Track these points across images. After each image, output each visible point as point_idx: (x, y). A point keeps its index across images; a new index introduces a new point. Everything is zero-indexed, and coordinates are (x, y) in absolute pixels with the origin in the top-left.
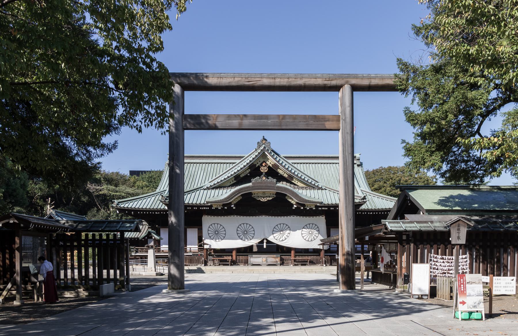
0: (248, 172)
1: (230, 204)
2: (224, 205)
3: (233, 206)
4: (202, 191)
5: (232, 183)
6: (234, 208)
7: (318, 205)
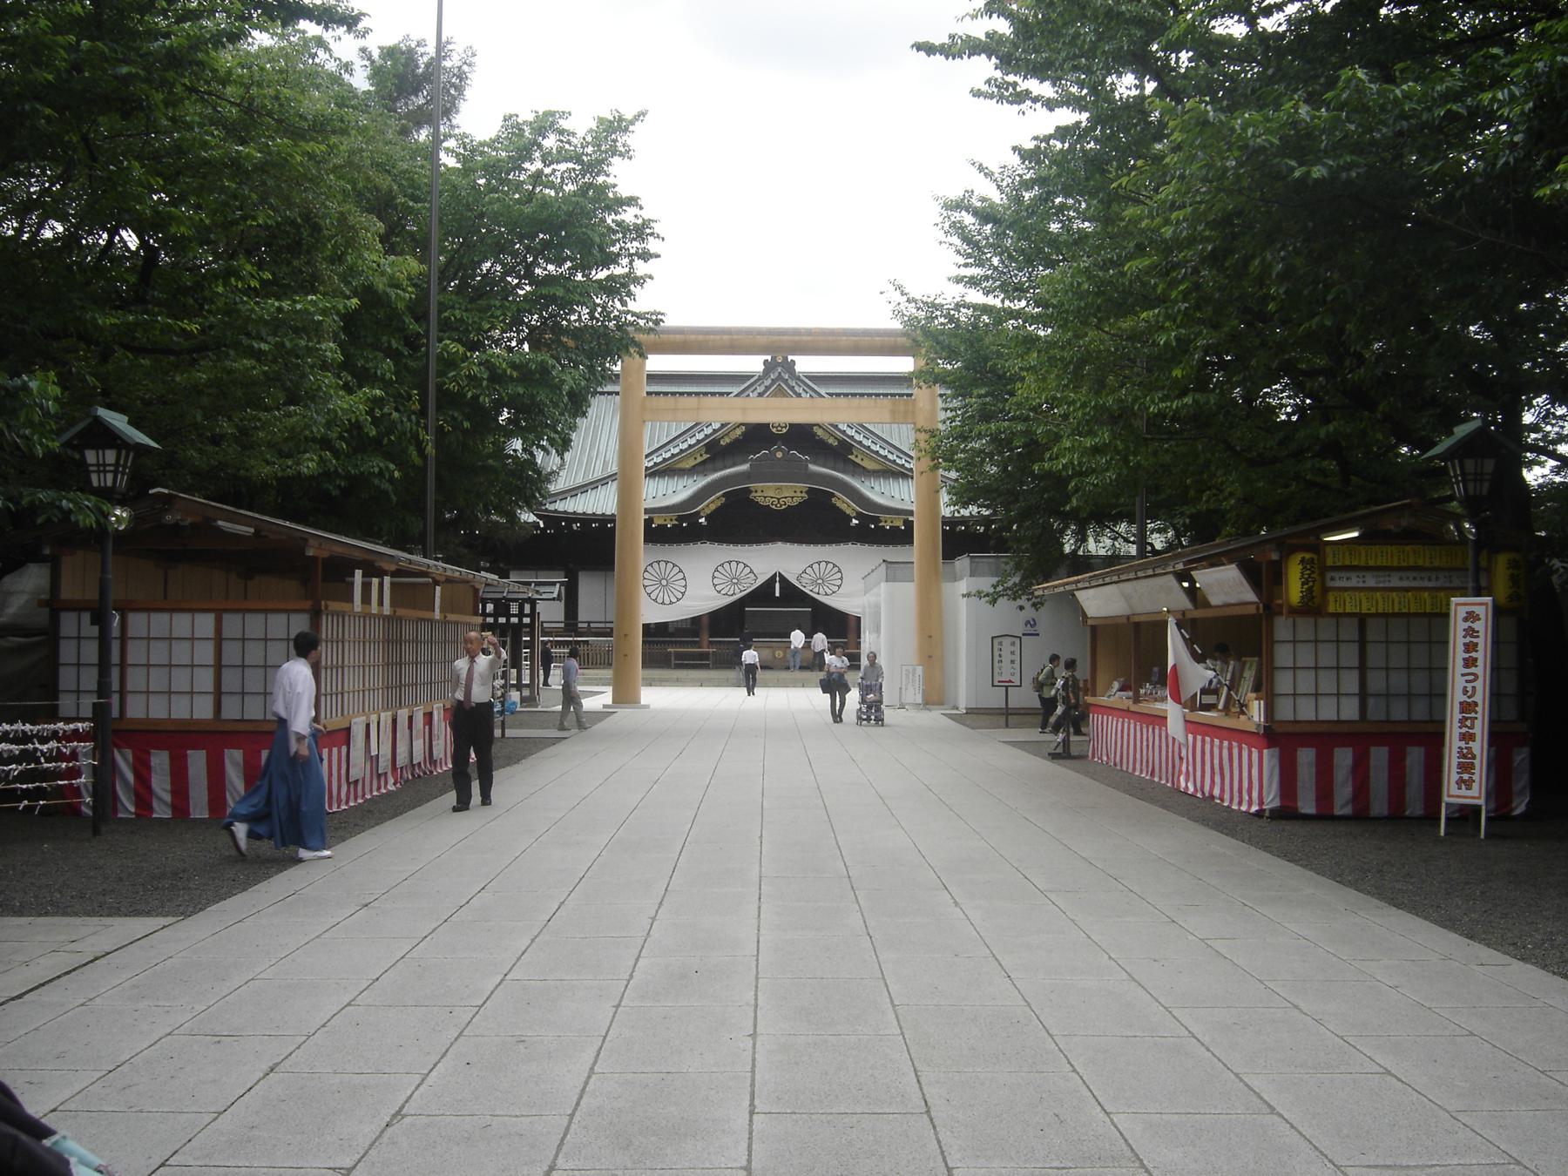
1: (698, 513)
2: (681, 519)
3: (702, 520)
5: (700, 459)
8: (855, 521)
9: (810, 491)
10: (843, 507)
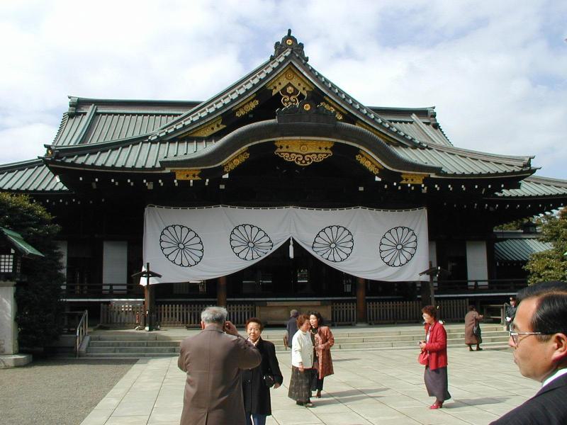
0: (253, 105)
1: (221, 168)
2: (204, 174)
4: (146, 146)
7: (433, 176)
8: (378, 179)
9: (336, 147)
10: (368, 164)
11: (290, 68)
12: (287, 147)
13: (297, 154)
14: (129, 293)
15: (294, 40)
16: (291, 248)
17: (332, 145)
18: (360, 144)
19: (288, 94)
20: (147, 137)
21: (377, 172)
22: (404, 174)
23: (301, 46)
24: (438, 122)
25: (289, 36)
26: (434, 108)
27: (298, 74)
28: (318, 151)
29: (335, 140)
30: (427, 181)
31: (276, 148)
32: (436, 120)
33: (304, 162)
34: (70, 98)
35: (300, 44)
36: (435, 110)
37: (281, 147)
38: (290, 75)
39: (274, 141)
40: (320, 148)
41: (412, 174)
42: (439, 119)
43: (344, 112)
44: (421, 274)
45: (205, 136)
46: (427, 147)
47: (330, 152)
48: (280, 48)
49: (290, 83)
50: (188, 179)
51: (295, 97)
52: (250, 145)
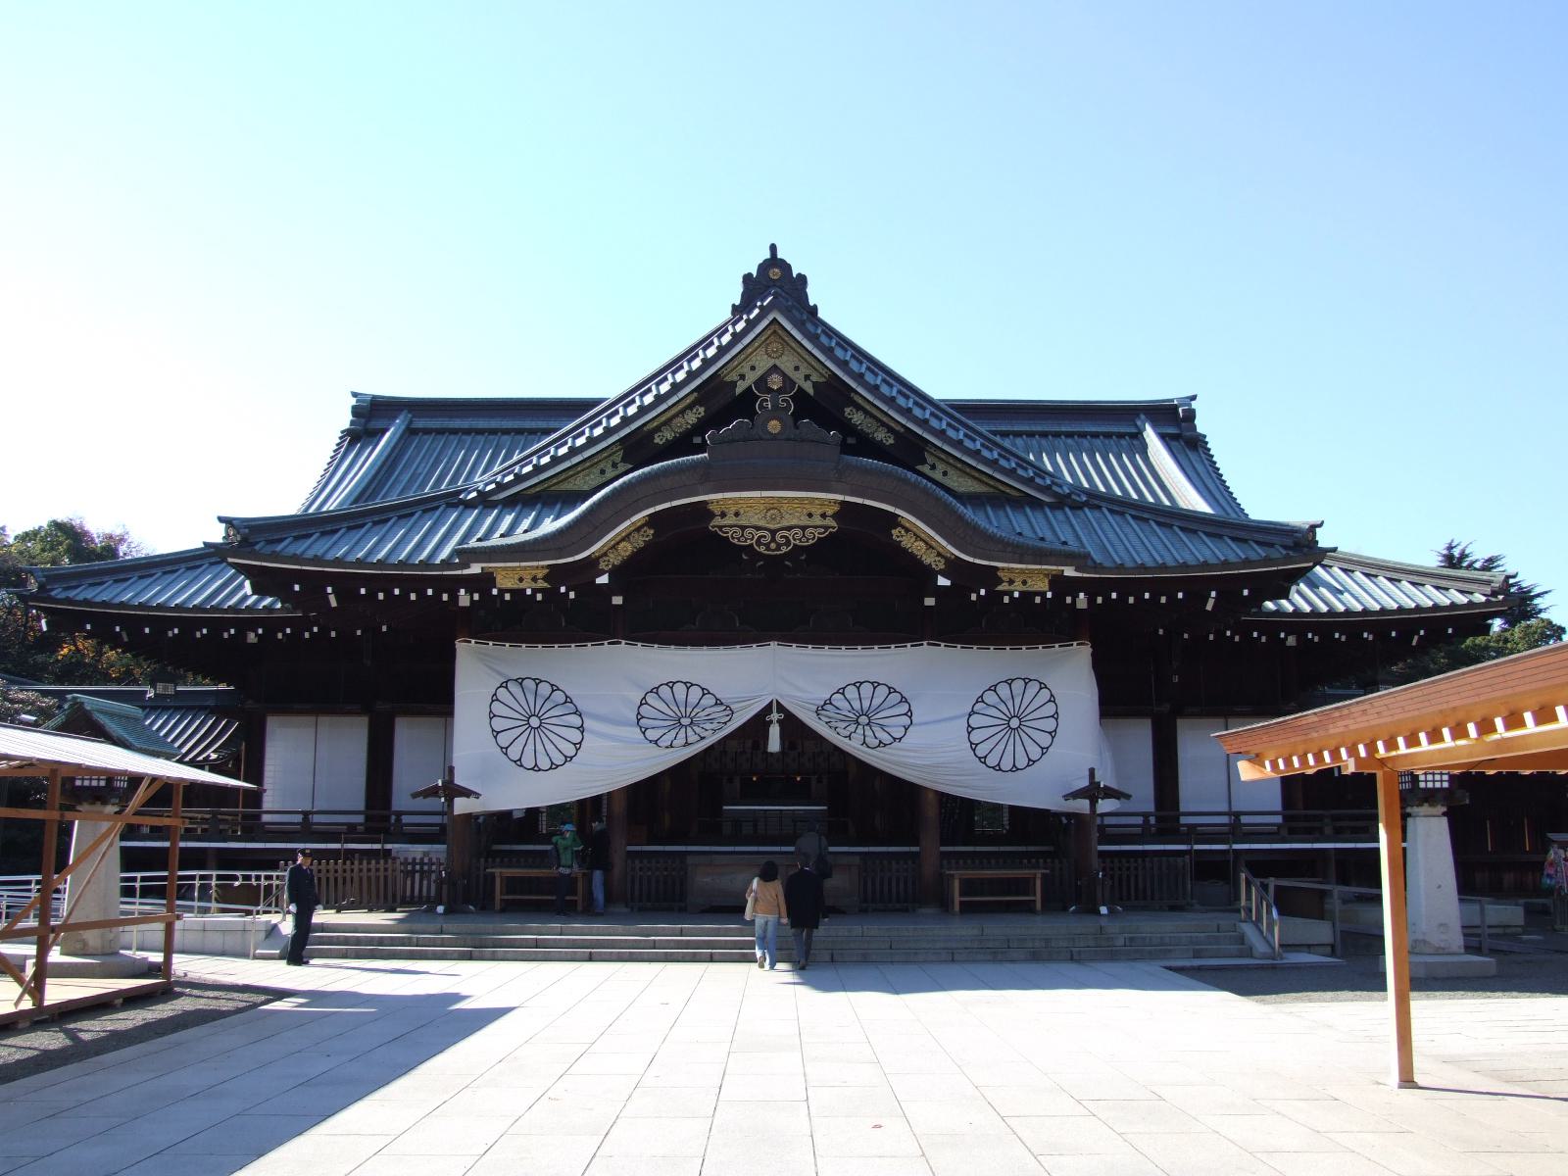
0: (692, 418)
1: (591, 565)
2: (555, 574)
3: (603, 580)
6: (617, 600)
7: (1069, 572)
8: (943, 581)
11: (775, 332)
12: (737, 514)
13: (758, 528)
14: (368, 830)
15: (786, 267)
16: (775, 732)
17: (837, 508)
18: (896, 506)
19: (770, 390)
20: (460, 492)
21: (942, 566)
22: (1003, 569)
23: (802, 279)
24: (1200, 429)
25: (774, 261)
26: (1194, 398)
27: (793, 345)
28: (805, 521)
29: (840, 497)
30: (1058, 583)
31: (711, 515)
32: (1194, 427)
33: (773, 546)
34: (355, 395)
35: (799, 275)
36: (1194, 405)
37: (723, 515)
38: (775, 346)
39: (705, 503)
40: (810, 515)
41: (1022, 571)
42: (1202, 425)
43: (898, 428)
44: (1067, 797)
45: (586, 488)
46: (1086, 504)
47: (834, 524)
48: (754, 287)
49: (775, 369)
50: (522, 586)
51: (786, 396)
52: (651, 510)
